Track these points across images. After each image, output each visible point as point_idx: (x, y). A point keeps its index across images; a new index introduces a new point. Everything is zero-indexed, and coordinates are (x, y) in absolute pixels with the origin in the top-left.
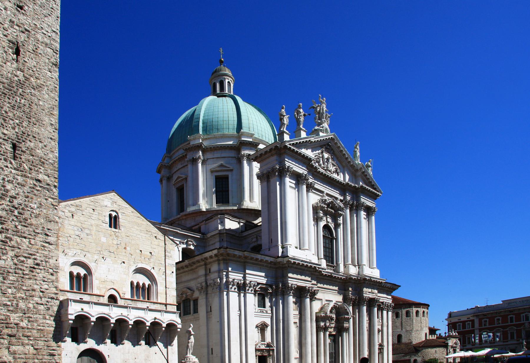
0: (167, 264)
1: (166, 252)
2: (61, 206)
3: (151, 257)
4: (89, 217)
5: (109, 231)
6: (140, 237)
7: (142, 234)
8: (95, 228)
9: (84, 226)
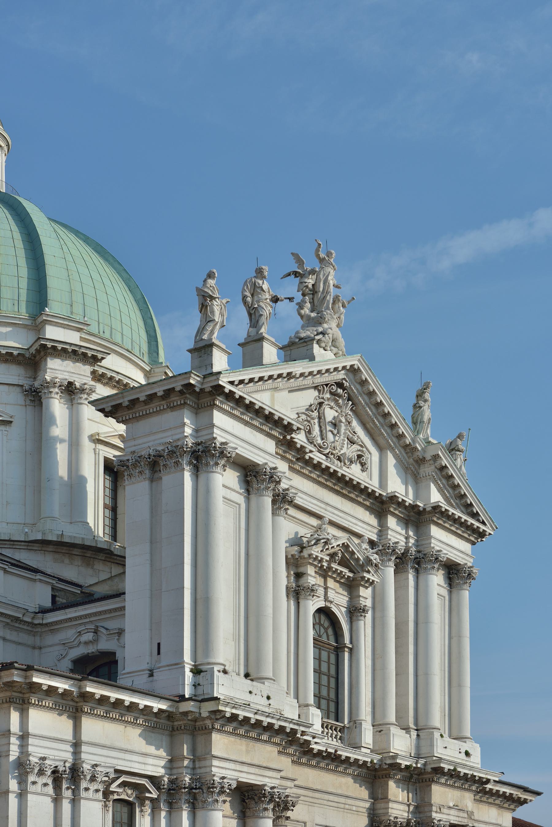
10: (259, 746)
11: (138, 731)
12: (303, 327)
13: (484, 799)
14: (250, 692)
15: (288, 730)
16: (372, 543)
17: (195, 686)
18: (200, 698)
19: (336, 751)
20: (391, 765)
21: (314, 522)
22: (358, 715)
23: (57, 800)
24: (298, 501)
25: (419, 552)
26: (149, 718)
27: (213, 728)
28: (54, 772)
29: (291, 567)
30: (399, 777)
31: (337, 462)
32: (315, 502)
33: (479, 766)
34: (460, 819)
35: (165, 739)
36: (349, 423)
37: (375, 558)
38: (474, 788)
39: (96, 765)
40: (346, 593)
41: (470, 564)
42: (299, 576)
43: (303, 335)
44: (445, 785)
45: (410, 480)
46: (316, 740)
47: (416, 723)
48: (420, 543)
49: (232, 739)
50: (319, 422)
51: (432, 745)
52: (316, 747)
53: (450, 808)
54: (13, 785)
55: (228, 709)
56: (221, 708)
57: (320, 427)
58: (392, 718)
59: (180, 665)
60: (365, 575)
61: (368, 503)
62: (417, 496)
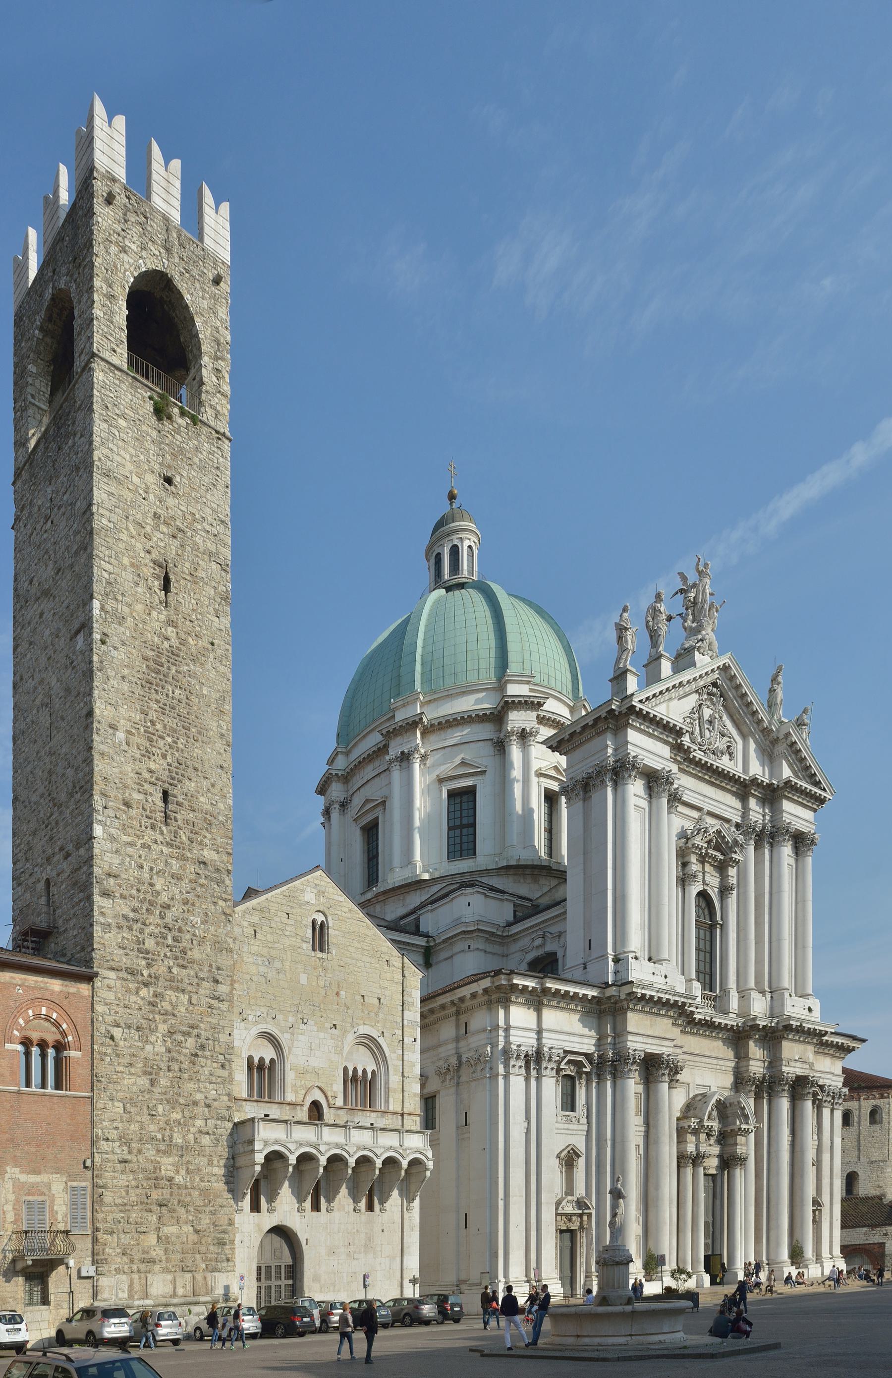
0: (406, 1022)
1: (405, 993)
2: (237, 915)
3: (379, 1008)
4: (281, 933)
5: (313, 958)
6: (363, 965)
7: (364, 958)
8: (289, 954)
9: (274, 953)
10: (659, 1020)
11: (578, 1016)
12: (687, 639)
13: (821, 1050)
14: (653, 974)
15: (680, 1004)
16: (738, 826)
17: (616, 973)
18: (619, 983)
19: (712, 1018)
20: (751, 1026)
21: (695, 814)
22: (726, 984)
23: (527, 1079)
24: (685, 798)
25: (773, 827)
26: (585, 1004)
27: (628, 1008)
28: (525, 1056)
29: (679, 858)
30: (757, 1037)
31: (712, 756)
32: (696, 796)
33: (819, 1020)
34: (803, 1071)
35: (595, 1021)
36: (721, 718)
37: (740, 839)
38: (814, 1041)
39: (552, 1048)
40: (717, 875)
41: (813, 832)
42: (685, 865)
43: (687, 646)
44: (793, 1040)
45: (767, 761)
46: (698, 1010)
47: (770, 987)
48: (774, 819)
49: (641, 1016)
50: (699, 722)
51: (783, 1005)
52: (697, 1017)
53: (796, 1060)
54: (501, 1069)
55: (639, 990)
56: (635, 990)
57: (700, 726)
58: (752, 984)
59: (604, 956)
60: (734, 856)
61: (734, 789)
62: (771, 776)
